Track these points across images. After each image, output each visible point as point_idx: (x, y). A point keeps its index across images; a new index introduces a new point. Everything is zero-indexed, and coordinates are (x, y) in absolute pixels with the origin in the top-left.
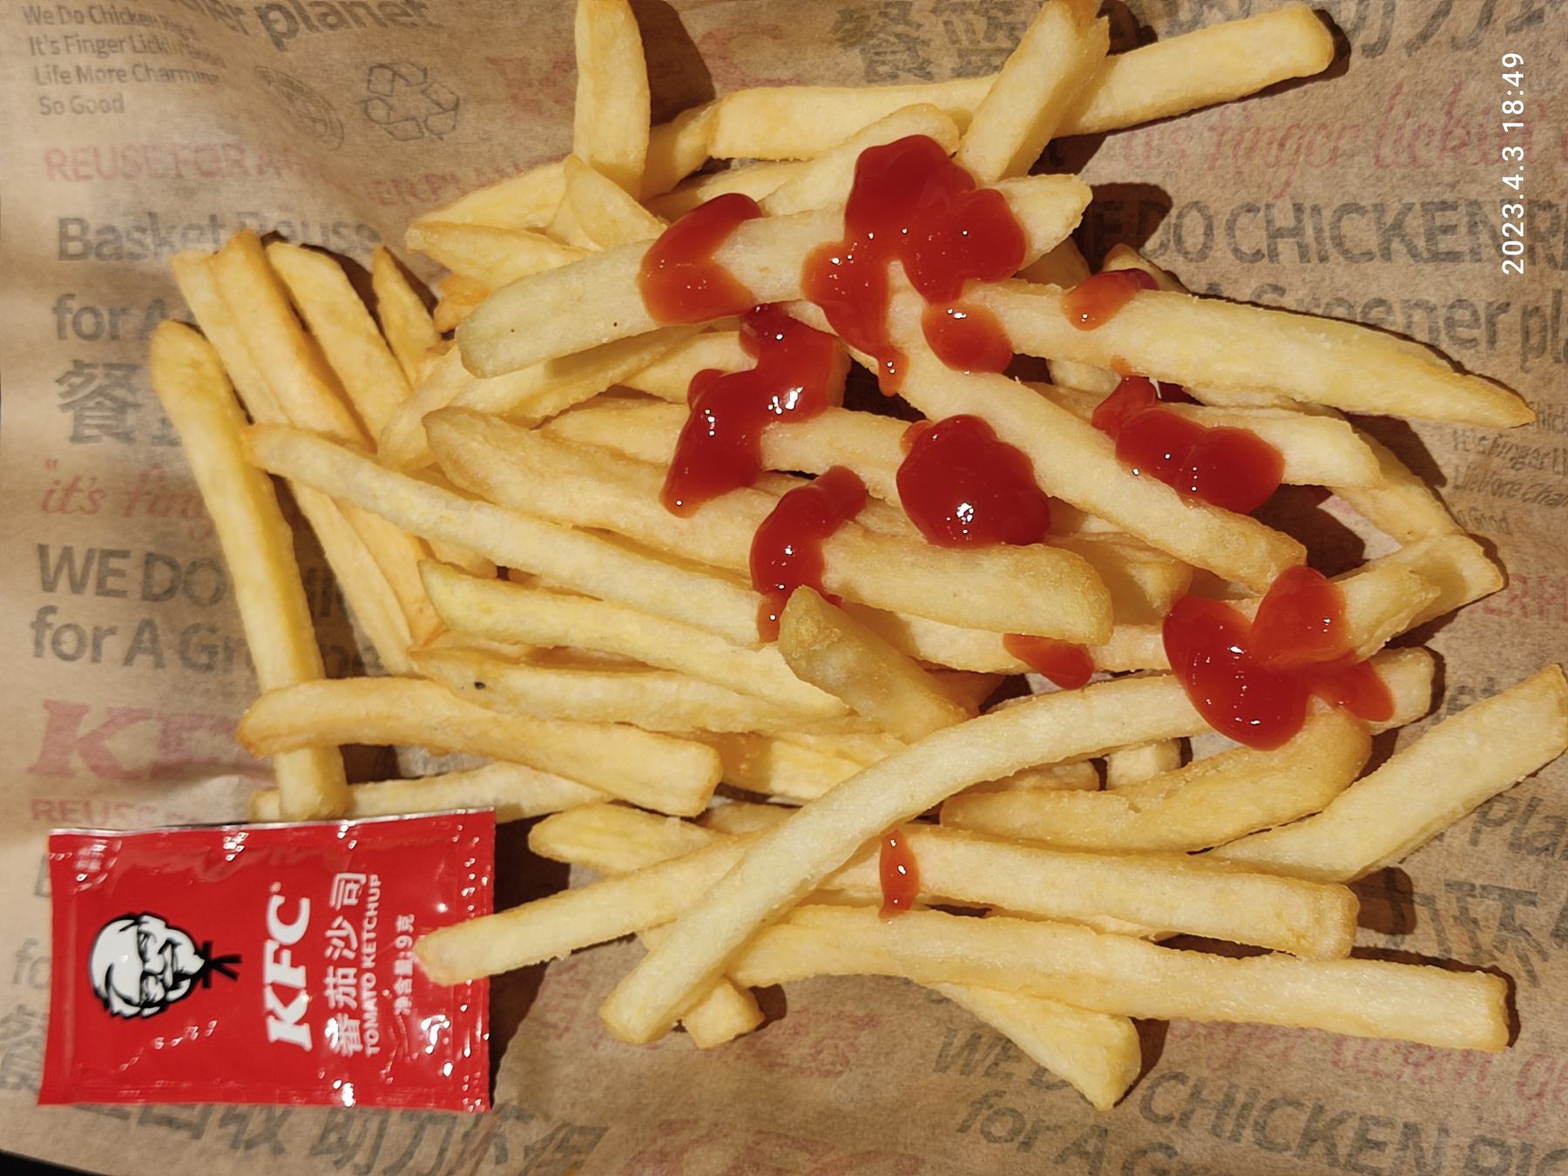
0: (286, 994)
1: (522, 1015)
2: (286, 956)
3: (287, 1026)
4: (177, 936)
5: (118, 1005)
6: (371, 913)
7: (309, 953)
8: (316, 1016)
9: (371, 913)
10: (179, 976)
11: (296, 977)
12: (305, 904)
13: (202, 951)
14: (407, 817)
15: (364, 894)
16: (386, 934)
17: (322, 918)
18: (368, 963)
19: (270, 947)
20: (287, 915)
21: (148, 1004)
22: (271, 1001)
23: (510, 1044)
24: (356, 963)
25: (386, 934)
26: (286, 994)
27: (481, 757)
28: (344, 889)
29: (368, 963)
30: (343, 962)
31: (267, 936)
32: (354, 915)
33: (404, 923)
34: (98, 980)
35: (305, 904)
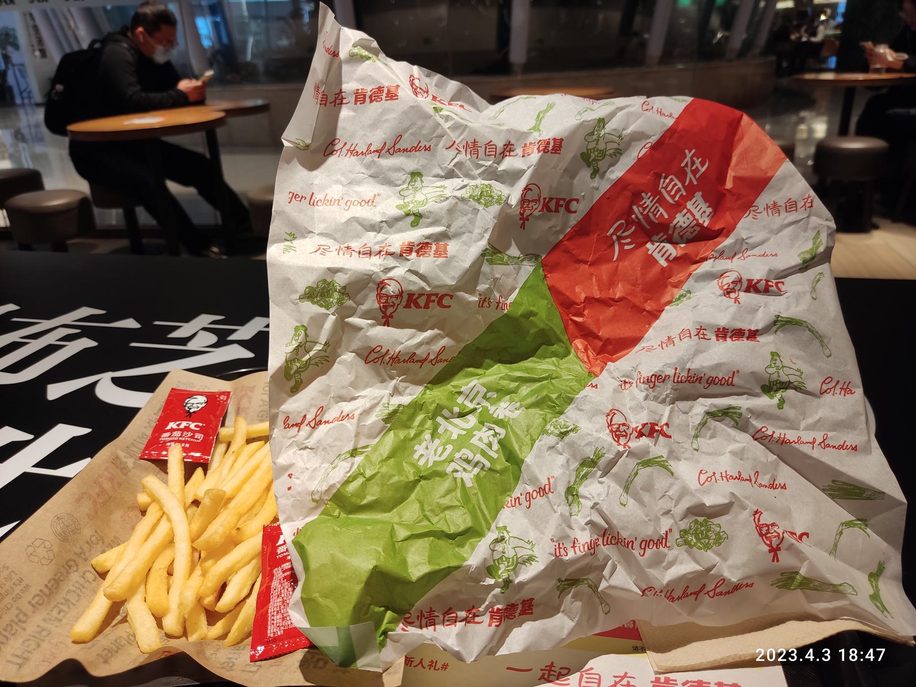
0: (178, 425)
1: (161, 469)
2: (188, 425)
3: (172, 425)
4: (199, 409)
5: (188, 400)
6: (192, 440)
7: (187, 429)
8: (172, 430)
9: (192, 440)
10: (190, 409)
11: (182, 427)
12: (198, 429)
13: (194, 412)
14: (213, 449)
15: (197, 439)
16: (185, 442)
17: (194, 432)
18: (180, 438)
19: (190, 423)
20: (196, 426)
21: (186, 404)
22: (178, 423)
23: (153, 465)
24: (181, 436)
25: (185, 442)
26: (178, 425)
27: (221, 463)
28: (200, 437)
29: (180, 438)
30: (182, 434)
31: (193, 422)
32: (192, 437)
33: (187, 445)
34: (195, 397)
35: (198, 429)
